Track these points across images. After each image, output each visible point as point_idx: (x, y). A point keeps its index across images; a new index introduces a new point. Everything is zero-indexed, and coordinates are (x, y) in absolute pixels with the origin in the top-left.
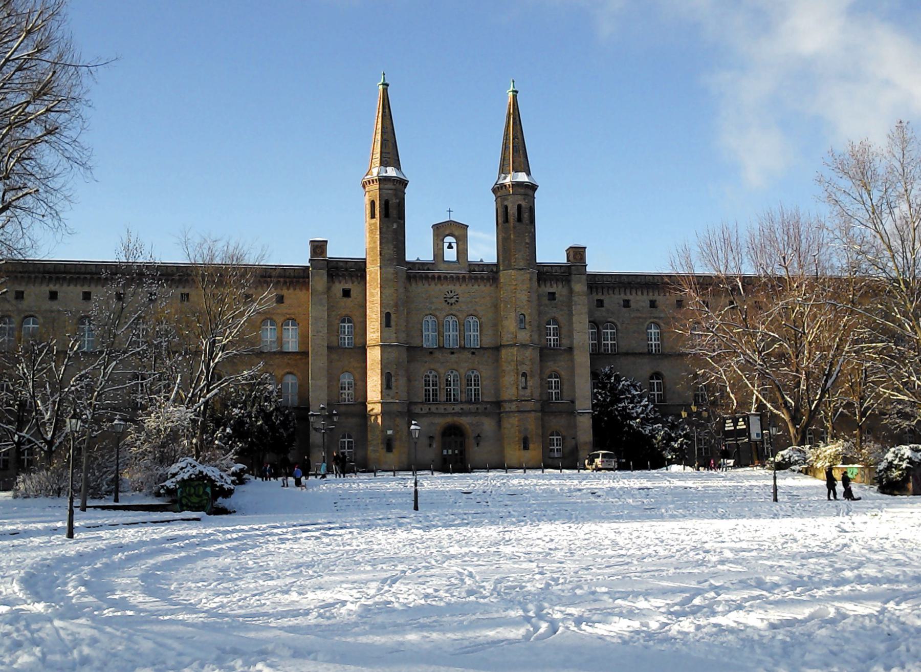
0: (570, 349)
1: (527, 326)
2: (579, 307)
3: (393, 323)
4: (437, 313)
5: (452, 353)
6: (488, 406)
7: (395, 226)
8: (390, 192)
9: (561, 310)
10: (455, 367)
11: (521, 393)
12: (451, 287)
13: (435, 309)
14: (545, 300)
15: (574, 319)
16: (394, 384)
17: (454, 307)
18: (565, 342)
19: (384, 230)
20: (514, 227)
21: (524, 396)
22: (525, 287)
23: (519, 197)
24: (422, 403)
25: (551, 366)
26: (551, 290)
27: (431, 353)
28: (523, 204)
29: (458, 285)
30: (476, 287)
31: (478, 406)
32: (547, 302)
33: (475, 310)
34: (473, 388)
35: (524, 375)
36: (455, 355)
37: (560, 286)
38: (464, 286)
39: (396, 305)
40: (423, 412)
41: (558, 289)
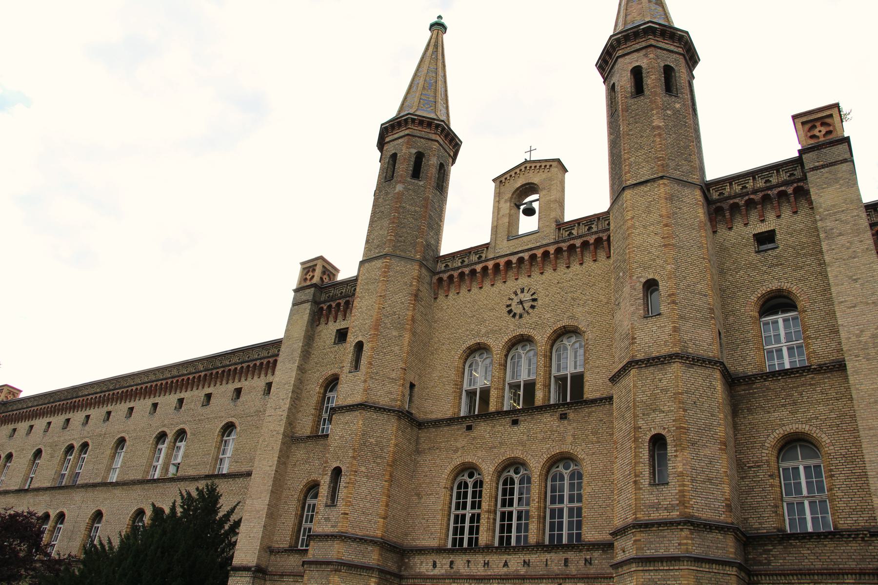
0: (839, 367)
1: (663, 309)
2: (842, 240)
3: (364, 361)
4: (490, 342)
5: (515, 422)
6: (596, 554)
7: (399, 188)
8: (400, 140)
9: (797, 268)
10: (518, 453)
11: (649, 496)
12: (523, 281)
13: (487, 334)
14: (749, 254)
15: (831, 272)
16: (342, 493)
17: (526, 318)
18: (821, 350)
19: (381, 200)
20: (626, 109)
21: (656, 507)
22: (655, 217)
23: (635, 55)
24: (440, 550)
25: (778, 419)
26: (763, 228)
27: (469, 428)
28: (643, 62)
29: (536, 275)
30: (575, 267)
31: (570, 555)
32: (754, 257)
33: (572, 317)
34: (566, 505)
35: (658, 442)
36: (522, 427)
37: (786, 213)
38: (549, 273)
39: (377, 325)
40: (436, 572)
41: (782, 222)
